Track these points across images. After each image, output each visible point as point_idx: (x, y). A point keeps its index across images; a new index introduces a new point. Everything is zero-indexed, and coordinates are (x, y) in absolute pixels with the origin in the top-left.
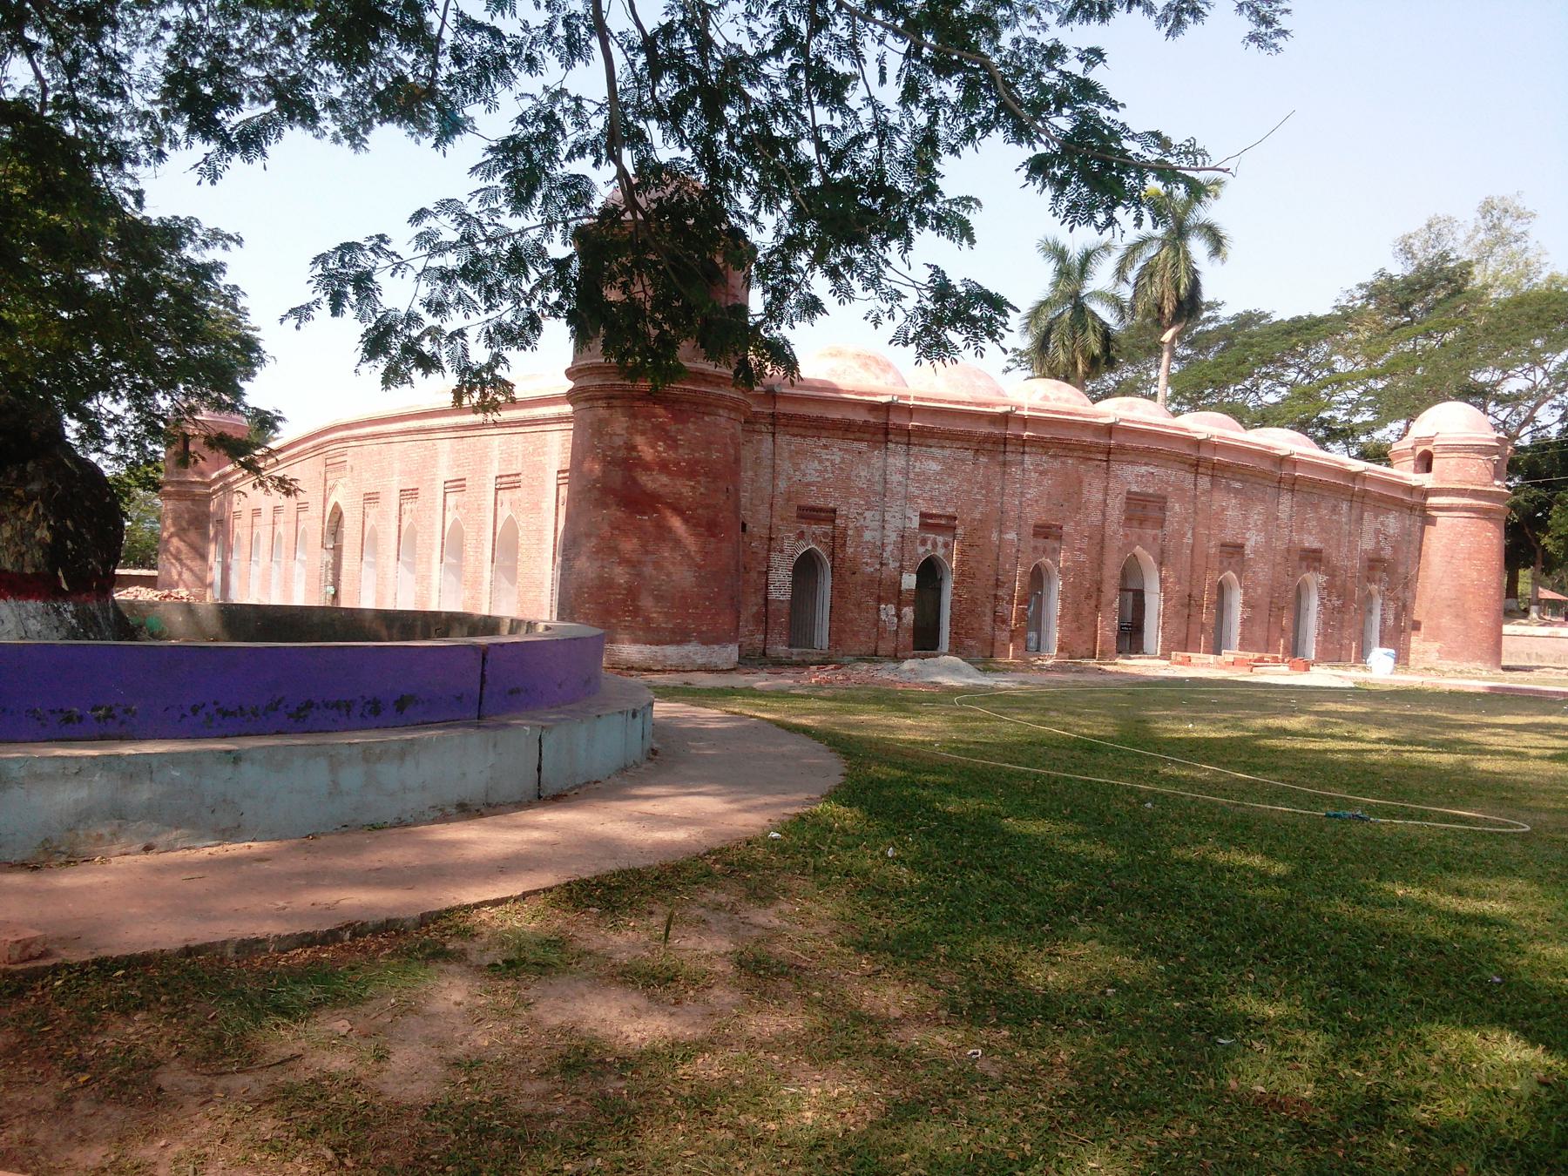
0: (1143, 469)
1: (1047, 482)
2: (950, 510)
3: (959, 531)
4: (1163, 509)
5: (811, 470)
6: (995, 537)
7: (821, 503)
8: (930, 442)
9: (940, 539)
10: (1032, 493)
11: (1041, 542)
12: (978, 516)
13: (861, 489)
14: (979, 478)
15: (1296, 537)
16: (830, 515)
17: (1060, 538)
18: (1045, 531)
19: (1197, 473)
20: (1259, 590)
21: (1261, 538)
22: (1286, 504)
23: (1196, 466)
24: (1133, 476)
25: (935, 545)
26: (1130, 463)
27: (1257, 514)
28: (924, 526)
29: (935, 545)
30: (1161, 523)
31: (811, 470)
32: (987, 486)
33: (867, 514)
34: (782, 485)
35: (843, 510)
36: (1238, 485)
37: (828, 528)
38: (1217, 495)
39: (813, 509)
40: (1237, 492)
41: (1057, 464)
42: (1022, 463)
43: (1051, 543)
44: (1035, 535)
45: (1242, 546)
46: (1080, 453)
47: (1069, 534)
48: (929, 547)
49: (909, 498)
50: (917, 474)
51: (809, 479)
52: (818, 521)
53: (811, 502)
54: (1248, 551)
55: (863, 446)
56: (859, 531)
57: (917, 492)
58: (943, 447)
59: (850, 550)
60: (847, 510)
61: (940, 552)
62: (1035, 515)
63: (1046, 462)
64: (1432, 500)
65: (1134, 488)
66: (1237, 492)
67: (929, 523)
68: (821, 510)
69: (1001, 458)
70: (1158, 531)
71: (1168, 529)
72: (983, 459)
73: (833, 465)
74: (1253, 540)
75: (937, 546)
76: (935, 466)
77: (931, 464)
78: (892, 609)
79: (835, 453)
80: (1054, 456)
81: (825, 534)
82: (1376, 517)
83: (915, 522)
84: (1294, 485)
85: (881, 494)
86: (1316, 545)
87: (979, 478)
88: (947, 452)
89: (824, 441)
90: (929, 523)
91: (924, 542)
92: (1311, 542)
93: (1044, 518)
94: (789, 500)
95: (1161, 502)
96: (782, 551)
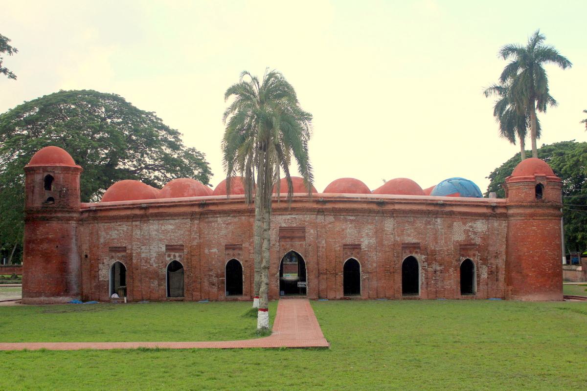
0: (289, 217)
1: (231, 227)
2: (181, 243)
3: (185, 251)
4: (304, 232)
5: (114, 234)
6: (206, 251)
7: (119, 245)
8: (167, 218)
9: (177, 254)
10: (223, 232)
11: (231, 252)
12: (196, 244)
13: (137, 239)
14: (195, 229)
15: (398, 239)
16: (124, 249)
17: (241, 249)
19: (325, 215)
20: (375, 265)
21: (373, 241)
22: (389, 224)
23: (320, 212)
24: (283, 220)
25: (175, 256)
26: (279, 215)
30: (304, 238)
31: (114, 234)
32: (200, 232)
33: (142, 247)
34: (102, 240)
35: (129, 247)
37: (124, 254)
39: (116, 248)
40: (351, 221)
41: (236, 220)
42: (217, 221)
43: (236, 252)
45: (360, 245)
46: (249, 214)
47: (245, 248)
48: (172, 257)
49: (161, 240)
51: (113, 237)
52: (119, 252)
54: (363, 247)
55: (138, 223)
56: (139, 254)
57: (163, 238)
58: (175, 219)
59: (134, 261)
60: (134, 247)
61: (178, 259)
62: (224, 242)
63: (229, 219)
64: (511, 212)
65: (284, 225)
66: (351, 221)
67: (170, 248)
68: (119, 248)
69: (207, 220)
70: (304, 243)
71: (308, 241)
72: (196, 222)
74: (365, 243)
76: (171, 227)
77: (170, 226)
78: (156, 282)
79: (124, 227)
81: (123, 256)
82: (465, 224)
83: (164, 249)
84: (393, 213)
85: (146, 241)
86: (415, 241)
87: (195, 229)
88: (177, 221)
89: (119, 223)
90: (170, 248)
91: (169, 256)
92: (412, 240)
95: (303, 229)
96: (103, 263)
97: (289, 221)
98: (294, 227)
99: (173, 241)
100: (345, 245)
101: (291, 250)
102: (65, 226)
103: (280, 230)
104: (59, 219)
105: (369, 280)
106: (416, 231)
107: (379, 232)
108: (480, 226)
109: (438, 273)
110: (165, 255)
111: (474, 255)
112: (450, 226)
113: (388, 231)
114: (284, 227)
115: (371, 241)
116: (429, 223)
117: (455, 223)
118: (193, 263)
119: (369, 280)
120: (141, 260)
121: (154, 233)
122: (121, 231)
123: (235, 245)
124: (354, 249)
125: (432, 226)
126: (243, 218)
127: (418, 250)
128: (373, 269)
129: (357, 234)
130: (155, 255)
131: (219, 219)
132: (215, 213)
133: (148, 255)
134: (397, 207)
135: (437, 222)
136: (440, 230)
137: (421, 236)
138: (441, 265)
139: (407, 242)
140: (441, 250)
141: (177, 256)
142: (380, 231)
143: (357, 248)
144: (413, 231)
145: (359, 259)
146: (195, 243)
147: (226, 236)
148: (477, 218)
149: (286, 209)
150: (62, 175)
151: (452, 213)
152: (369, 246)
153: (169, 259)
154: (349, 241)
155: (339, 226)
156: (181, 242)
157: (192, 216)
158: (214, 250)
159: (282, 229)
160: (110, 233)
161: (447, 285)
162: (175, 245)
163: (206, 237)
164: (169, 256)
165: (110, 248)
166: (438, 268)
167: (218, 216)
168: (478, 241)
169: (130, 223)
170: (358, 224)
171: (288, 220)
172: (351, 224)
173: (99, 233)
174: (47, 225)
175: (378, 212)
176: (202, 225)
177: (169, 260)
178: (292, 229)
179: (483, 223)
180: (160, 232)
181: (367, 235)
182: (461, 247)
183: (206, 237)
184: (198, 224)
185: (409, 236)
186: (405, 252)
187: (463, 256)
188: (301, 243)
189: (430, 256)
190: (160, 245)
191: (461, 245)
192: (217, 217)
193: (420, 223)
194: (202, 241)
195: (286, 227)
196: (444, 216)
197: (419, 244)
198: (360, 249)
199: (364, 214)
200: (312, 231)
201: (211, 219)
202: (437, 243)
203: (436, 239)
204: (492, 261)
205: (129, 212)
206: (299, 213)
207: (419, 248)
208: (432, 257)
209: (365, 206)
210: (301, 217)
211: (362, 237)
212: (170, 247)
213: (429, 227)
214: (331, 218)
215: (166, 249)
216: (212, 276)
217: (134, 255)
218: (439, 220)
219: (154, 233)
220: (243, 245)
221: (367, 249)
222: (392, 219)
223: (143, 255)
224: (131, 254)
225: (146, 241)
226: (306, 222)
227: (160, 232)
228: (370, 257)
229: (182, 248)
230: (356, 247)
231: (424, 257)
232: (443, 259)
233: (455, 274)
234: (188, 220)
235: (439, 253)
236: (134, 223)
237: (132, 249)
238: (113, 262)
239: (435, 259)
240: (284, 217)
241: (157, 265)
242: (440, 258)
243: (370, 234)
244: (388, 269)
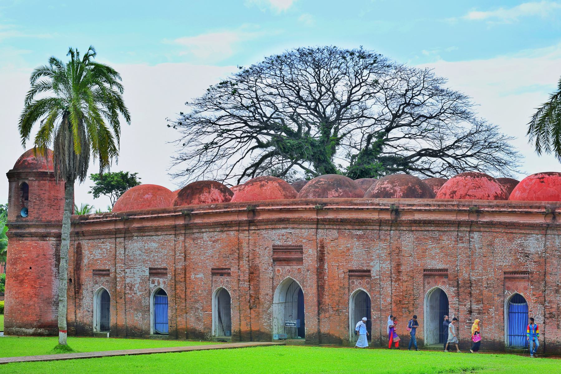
0: (284, 231)
1: (218, 246)
3: (169, 276)
4: (302, 253)
6: (193, 277)
7: (102, 267)
9: (161, 280)
10: (210, 252)
13: (121, 259)
15: (419, 263)
17: (229, 274)
18: (218, 272)
20: (389, 300)
21: (387, 266)
22: (408, 241)
24: (277, 236)
25: (159, 283)
26: (273, 229)
27: (380, 248)
28: (150, 273)
29: (159, 283)
30: (300, 261)
33: (126, 270)
34: (85, 261)
36: (360, 233)
37: (107, 278)
38: (342, 241)
39: (100, 270)
40: (359, 237)
41: (224, 235)
44: (213, 274)
45: (369, 271)
46: (237, 228)
48: (156, 284)
49: (144, 261)
50: (146, 250)
53: (98, 267)
54: (373, 274)
55: (122, 240)
57: (147, 258)
59: (118, 288)
61: (162, 286)
63: (217, 235)
65: (278, 243)
67: (155, 272)
73: (107, 250)
75: (162, 283)
76: (155, 245)
80: (222, 231)
81: (107, 281)
82: (510, 240)
83: (147, 273)
89: (102, 240)
90: (155, 272)
91: (153, 282)
93: (218, 265)
94: (89, 267)
95: (299, 249)
96: (87, 289)
97: (284, 237)
98: (290, 246)
99: (157, 263)
100: (350, 271)
101: (288, 277)
102: (41, 243)
103: (273, 249)
104: (32, 235)
105: (381, 321)
106: (442, 252)
107: (396, 253)
109: (475, 314)
110: (149, 280)
111: (526, 289)
112: (491, 244)
113: (406, 250)
114: (278, 246)
115: (384, 265)
116: (459, 239)
117: (497, 240)
118: (178, 291)
119: (381, 321)
120: (125, 287)
121: (138, 252)
122: (104, 250)
123: (222, 269)
124: (362, 277)
125: (465, 245)
126: (232, 233)
127: (445, 280)
128: (386, 306)
129: (366, 257)
130: (139, 280)
131: (205, 234)
132: (200, 227)
133: (132, 279)
134: (417, 217)
135: (473, 238)
136: (478, 251)
138: (478, 301)
139: (429, 267)
140: (479, 280)
141: (161, 282)
142: (397, 251)
143: (366, 276)
145: (369, 291)
146: (180, 266)
147: (212, 256)
148: (528, 232)
149: (281, 221)
150: (37, 182)
151: (491, 224)
152: (381, 273)
153: (153, 285)
154: (354, 265)
155: (344, 243)
156: (165, 265)
157: (115, 234)
158: (201, 276)
159: (276, 249)
160: (94, 252)
161: (487, 333)
162: (159, 269)
163: (193, 259)
164: (153, 282)
165: (93, 270)
166: (475, 307)
167: (203, 230)
168: (531, 267)
169: (113, 240)
170: (366, 241)
171: (283, 235)
172: (358, 241)
173: (83, 251)
174: (20, 242)
176: (189, 242)
177: (153, 287)
178: (287, 249)
179: (537, 239)
180: (144, 251)
181: (379, 256)
182: (507, 276)
183: (193, 259)
184: (184, 242)
185: (433, 258)
186: (428, 283)
187: (508, 288)
188: (299, 267)
189: (462, 289)
190: (144, 268)
191: (505, 273)
192: (203, 232)
193: (448, 240)
194: (187, 263)
195: (280, 246)
196: (482, 229)
197: (446, 270)
198: (370, 276)
199: (374, 227)
200: (310, 251)
201: (196, 235)
202: (473, 269)
203: (471, 264)
204: (552, 299)
205: (112, 227)
206: (296, 226)
207: (446, 276)
208: (465, 288)
209: (375, 216)
210: (297, 231)
211: (372, 260)
212: (154, 271)
213: (461, 245)
214: (334, 233)
215: (150, 273)
216: (198, 309)
217: (118, 279)
218: (476, 235)
219: (138, 252)
220: (232, 270)
221: (378, 277)
222: (411, 234)
223: (128, 281)
224: (116, 278)
225: (128, 263)
226: (304, 239)
227: (144, 251)
228: (383, 288)
229: (165, 271)
230: (364, 274)
231: (454, 289)
232: (481, 293)
233: (497, 317)
234: (172, 237)
235: (476, 283)
236: (118, 240)
237: (115, 272)
238: (97, 288)
239: (470, 293)
240: (278, 231)
241: (141, 293)
242: (478, 291)
243: (383, 255)
244: (407, 306)
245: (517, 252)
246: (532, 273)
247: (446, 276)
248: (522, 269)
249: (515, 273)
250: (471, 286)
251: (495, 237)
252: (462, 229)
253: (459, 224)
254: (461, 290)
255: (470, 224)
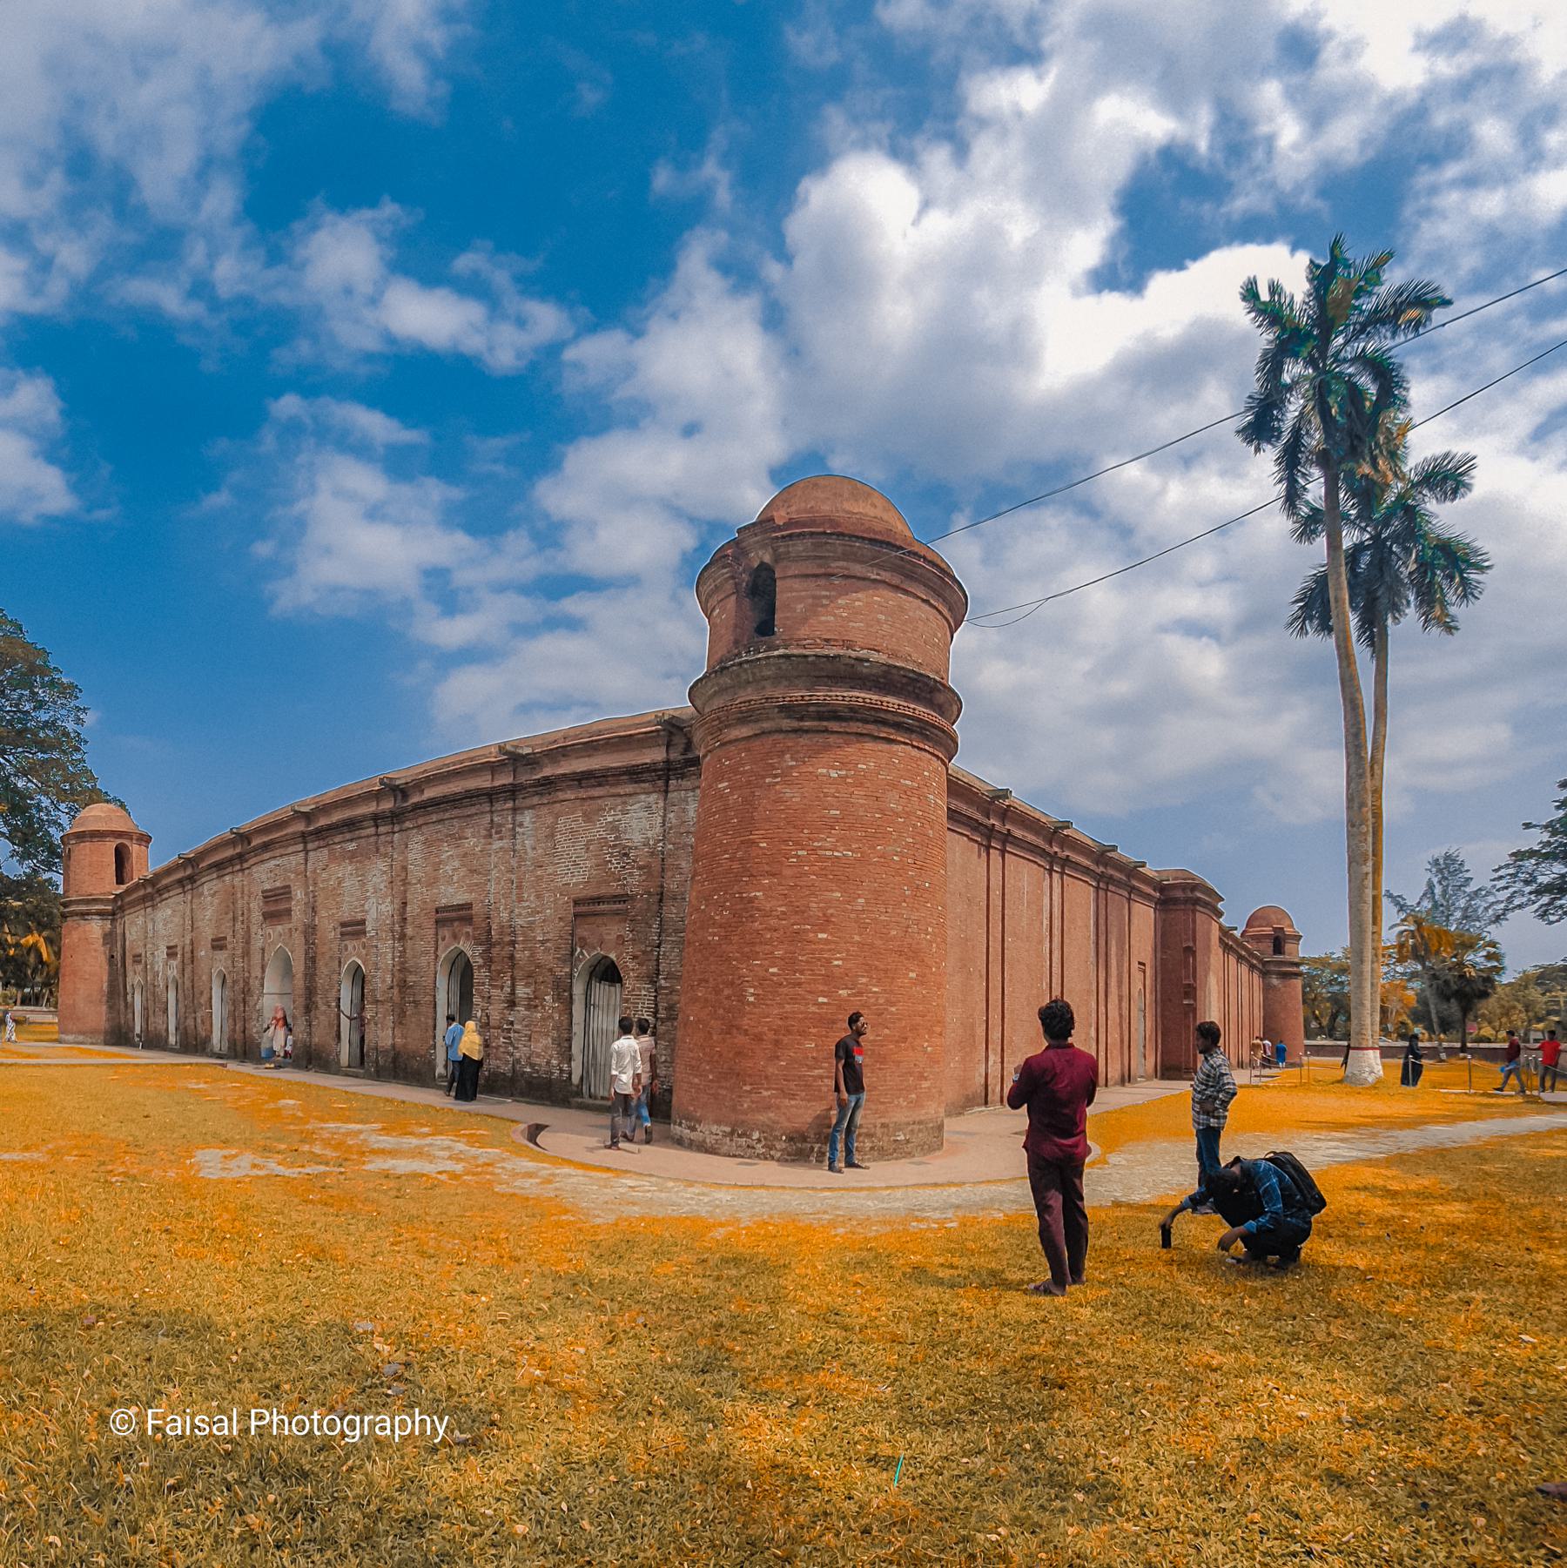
27: (378, 871)
36: (352, 846)
40: (352, 856)
107: (400, 881)
108: (640, 820)
135: (521, 825)
137: (476, 879)
144: (456, 864)
151: (549, 784)
175: (395, 817)
185: (450, 881)
191: (576, 903)
207: (468, 920)
235: (524, 934)
245: (603, 842)
246: (632, 898)
247: (468, 920)
248: (614, 888)
249: (598, 900)
250: (513, 943)
251: (557, 816)
252: (497, 806)
253: (491, 795)
254: (495, 951)
255: (512, 792)
